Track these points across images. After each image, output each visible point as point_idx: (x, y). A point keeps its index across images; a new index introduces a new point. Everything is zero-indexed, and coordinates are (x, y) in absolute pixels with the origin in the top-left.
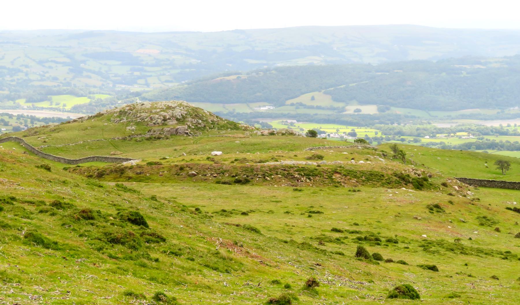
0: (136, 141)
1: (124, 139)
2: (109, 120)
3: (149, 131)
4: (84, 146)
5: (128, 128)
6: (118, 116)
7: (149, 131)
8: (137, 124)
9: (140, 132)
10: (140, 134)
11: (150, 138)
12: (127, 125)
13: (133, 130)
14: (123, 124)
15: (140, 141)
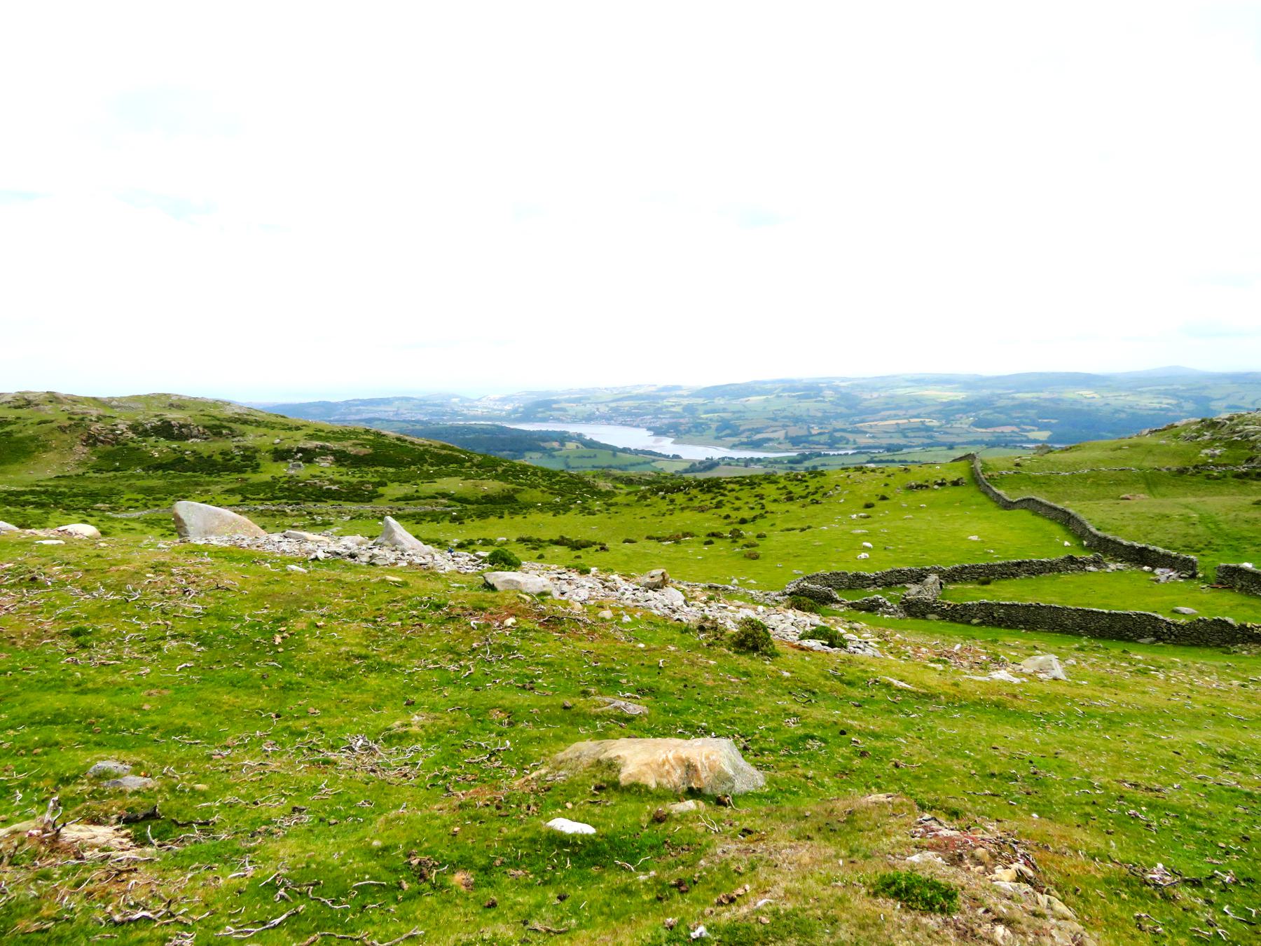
0: (1208, 477)
1: (1182, 471)
2: (1176, 436)
3: (1251, 460)
4: (1087, 477)
5: (1207, 451)
6: (1198, 430)
7: (1251, 460)
8: (1231, 445)
9: (1225, 462)
10: (1225, 465)
11: (1246, 474)
12: (1205, 447)
13: (1213, 456)
14: (1199, 443)
15: (1217, 478)
